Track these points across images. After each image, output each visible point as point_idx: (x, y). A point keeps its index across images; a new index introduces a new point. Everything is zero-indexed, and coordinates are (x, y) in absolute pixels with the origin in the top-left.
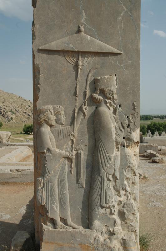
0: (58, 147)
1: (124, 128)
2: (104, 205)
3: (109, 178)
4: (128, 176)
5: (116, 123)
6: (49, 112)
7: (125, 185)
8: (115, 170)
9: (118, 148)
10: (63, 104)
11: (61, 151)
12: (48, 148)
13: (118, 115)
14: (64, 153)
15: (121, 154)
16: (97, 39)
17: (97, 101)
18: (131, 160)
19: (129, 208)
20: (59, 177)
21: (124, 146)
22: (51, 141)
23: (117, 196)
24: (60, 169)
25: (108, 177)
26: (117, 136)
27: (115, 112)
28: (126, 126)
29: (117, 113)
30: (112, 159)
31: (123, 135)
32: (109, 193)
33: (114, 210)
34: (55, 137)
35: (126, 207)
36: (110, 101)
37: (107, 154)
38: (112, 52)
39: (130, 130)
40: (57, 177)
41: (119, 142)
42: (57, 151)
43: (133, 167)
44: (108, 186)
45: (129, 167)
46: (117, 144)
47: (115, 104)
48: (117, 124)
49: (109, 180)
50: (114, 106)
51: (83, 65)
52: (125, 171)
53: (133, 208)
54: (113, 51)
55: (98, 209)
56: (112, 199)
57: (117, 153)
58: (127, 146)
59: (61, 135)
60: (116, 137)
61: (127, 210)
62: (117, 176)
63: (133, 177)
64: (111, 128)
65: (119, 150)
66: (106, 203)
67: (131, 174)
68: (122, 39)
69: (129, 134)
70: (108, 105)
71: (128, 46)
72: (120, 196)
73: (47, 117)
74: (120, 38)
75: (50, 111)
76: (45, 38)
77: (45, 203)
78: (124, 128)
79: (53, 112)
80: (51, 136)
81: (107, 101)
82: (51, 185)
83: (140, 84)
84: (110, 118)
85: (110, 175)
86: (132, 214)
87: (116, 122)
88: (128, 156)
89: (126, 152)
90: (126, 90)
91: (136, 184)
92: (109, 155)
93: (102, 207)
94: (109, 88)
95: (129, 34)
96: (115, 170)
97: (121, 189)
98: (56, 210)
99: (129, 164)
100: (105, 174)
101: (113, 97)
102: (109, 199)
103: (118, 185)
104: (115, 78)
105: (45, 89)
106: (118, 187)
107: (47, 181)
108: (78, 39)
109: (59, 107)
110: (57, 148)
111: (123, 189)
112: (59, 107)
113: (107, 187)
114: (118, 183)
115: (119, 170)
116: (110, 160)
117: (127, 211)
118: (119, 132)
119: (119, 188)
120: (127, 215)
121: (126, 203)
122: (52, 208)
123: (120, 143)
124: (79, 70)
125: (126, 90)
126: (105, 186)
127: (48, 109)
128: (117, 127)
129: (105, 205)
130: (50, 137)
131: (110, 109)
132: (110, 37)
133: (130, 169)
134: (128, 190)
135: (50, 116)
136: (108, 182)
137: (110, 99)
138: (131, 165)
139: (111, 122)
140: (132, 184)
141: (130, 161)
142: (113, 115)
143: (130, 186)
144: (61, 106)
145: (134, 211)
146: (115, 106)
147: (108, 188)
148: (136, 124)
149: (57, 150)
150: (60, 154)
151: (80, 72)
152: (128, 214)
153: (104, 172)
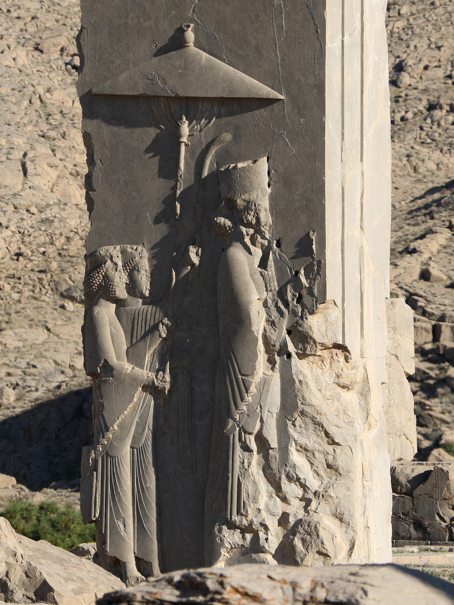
0: (129, 360)
1: (286, 305)
2: (233, 517)
3: (248, 442)
4: (303, 441)
5: (267, 290)
6: (109, 262)
7: (294, 467)
8: (262, 421)
9: (271, 361)
10: (146, 243)
11: (137, 369)
12: (106, 362)
13: (273, 268)
14: (143, 375)
15: (281, 376)
16: (224, 61)
17: (220, 230)
18: (307, 395)
19: (309, 537)
20: (133, 442)
21: (289, 356)
22: (113, 341)
23: (278, 499)
24: (136, 419)
25: (245, 439)
26: (268, 328)
27: (263, 264)
28: (293, 300)
29: (271, 262)
30: (253, 389)
31: (285, 324)
32: (247, 486)
33: (267, 539)
34: (125, 331)
35: (300, 533)
36: (252, 231)
37: (240, 377)
38: (256, 97)
39: (303, 311)
40: (129, 441)
41: (272, 343)
42: (127, 369)
43: (315, 415)
44: (246, 465)
45: (303, 413)
46: (268, 351)
47: (264, 238)
48: (270, 294)
49: (246, 448)
50: (263, 245)
51: (192, 133)
52: (294, 426)
53: (318, 536)
54: (259, 93)
55: (220, 531)
56: (255, 501)
57: (270, 372)
58: (303, 356)
59: (139, 326)
60: (265, 330)
61: (304, 541)
62: (269, 438)
63: (330, 449)
64: (249, 302)
65: (277, 366)
66: (239, 512)
67: (314, 438)
68: (283, 60)
69: (300, 321)
70: (247, 240)
71: (296, 78)
72: (284, 500)
73: (106, 277)
74: (277, 55)
75: (112, 261)
76: (104, 64)
77: (97, 515)
78: (286, 305)
79: (120, 264)
80: (115, 328)
81: (245, 233)
82: (112, 464)
83: (324, 182)
84: (248, 277)
85: (250, 434)
86: (319, 553)
87: (266, 286)
88: (300, 382)
89: (293, 372)
90: (291, 198)
91: (341, 471)
92: (244, 377)
93: (232, 526)
94: (246, 197)
95: (299, 43)
96: (262, 421)
97: (283, 477)
98: (123, 534)
99: (301, 407)
100: (237, 433)
101: (258, 219)
102: (247, 502)
103: (274, 465)
104: (265, 167)
105: (104, 202)
106: (276, 471)
107: (103, 451)
108: (178, 62)
109: (136, 250)
110: (129, 360)
111: (289, 478)
112: (136, 250)
113: (243, 467)
114: (276, 458)
115: (278, 420)
116: (247, 392)
117: (303, 545)
118: (275, 314)
119: (278, 475)
120: (302, 555)
121: (301, 520)
122: (114, 527)
123: (278, 347)
124: (183, 148)
125: (291, 198)
126: (237, 464)
127: (108, 254)
128: (270, 302)
129: (236, 518)
130: (111, 331)
131: (250, 253)
132: (256, 55)
133: (308, 420)
134: (307, 484)
135: (111, 272)
136: (246, 454)
137: (249, 225)
138: (307, 409)
139: (252, 287)
140: (328, 470)
141: (303, 397)
142: (260, 269)
143: (322, 473)
144: (140, 248)
145: (322, 543)
146: (266, 243)
147: (245, 470)
148: (316, 291)
149: (128, 367)
150: (134, 379)
151: (186, 152)
152: (304, 551)
153: (234, 425)
